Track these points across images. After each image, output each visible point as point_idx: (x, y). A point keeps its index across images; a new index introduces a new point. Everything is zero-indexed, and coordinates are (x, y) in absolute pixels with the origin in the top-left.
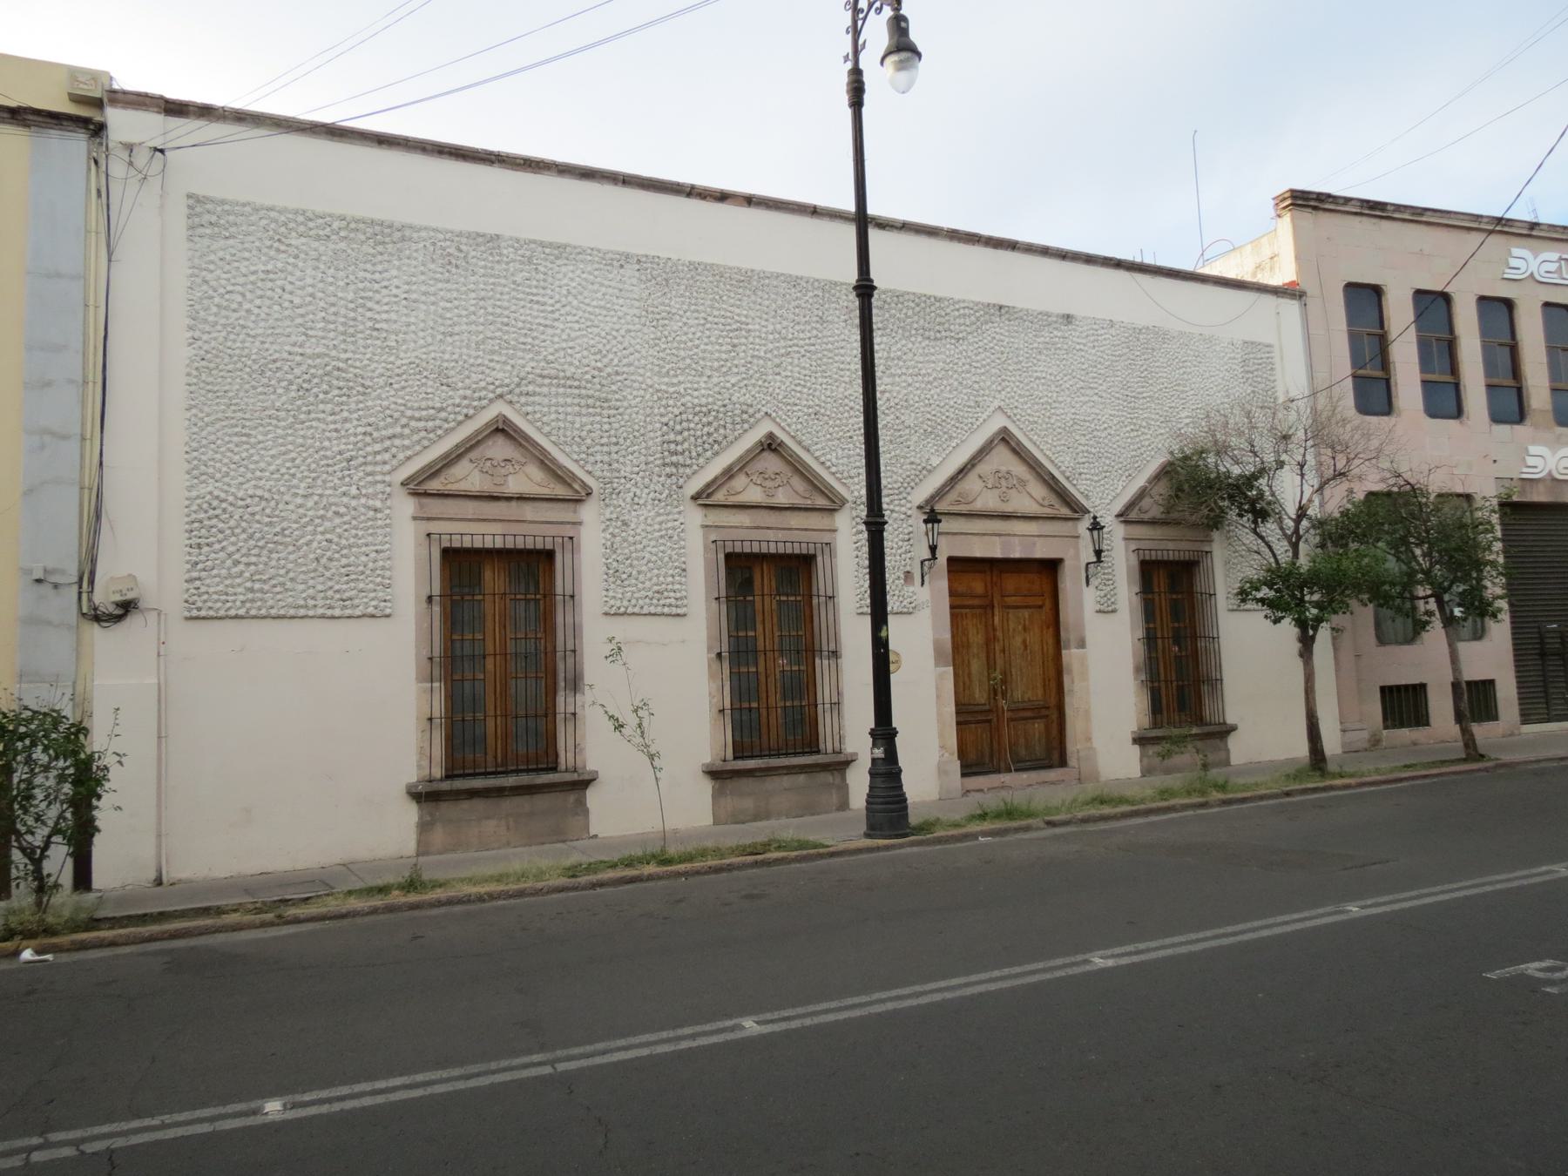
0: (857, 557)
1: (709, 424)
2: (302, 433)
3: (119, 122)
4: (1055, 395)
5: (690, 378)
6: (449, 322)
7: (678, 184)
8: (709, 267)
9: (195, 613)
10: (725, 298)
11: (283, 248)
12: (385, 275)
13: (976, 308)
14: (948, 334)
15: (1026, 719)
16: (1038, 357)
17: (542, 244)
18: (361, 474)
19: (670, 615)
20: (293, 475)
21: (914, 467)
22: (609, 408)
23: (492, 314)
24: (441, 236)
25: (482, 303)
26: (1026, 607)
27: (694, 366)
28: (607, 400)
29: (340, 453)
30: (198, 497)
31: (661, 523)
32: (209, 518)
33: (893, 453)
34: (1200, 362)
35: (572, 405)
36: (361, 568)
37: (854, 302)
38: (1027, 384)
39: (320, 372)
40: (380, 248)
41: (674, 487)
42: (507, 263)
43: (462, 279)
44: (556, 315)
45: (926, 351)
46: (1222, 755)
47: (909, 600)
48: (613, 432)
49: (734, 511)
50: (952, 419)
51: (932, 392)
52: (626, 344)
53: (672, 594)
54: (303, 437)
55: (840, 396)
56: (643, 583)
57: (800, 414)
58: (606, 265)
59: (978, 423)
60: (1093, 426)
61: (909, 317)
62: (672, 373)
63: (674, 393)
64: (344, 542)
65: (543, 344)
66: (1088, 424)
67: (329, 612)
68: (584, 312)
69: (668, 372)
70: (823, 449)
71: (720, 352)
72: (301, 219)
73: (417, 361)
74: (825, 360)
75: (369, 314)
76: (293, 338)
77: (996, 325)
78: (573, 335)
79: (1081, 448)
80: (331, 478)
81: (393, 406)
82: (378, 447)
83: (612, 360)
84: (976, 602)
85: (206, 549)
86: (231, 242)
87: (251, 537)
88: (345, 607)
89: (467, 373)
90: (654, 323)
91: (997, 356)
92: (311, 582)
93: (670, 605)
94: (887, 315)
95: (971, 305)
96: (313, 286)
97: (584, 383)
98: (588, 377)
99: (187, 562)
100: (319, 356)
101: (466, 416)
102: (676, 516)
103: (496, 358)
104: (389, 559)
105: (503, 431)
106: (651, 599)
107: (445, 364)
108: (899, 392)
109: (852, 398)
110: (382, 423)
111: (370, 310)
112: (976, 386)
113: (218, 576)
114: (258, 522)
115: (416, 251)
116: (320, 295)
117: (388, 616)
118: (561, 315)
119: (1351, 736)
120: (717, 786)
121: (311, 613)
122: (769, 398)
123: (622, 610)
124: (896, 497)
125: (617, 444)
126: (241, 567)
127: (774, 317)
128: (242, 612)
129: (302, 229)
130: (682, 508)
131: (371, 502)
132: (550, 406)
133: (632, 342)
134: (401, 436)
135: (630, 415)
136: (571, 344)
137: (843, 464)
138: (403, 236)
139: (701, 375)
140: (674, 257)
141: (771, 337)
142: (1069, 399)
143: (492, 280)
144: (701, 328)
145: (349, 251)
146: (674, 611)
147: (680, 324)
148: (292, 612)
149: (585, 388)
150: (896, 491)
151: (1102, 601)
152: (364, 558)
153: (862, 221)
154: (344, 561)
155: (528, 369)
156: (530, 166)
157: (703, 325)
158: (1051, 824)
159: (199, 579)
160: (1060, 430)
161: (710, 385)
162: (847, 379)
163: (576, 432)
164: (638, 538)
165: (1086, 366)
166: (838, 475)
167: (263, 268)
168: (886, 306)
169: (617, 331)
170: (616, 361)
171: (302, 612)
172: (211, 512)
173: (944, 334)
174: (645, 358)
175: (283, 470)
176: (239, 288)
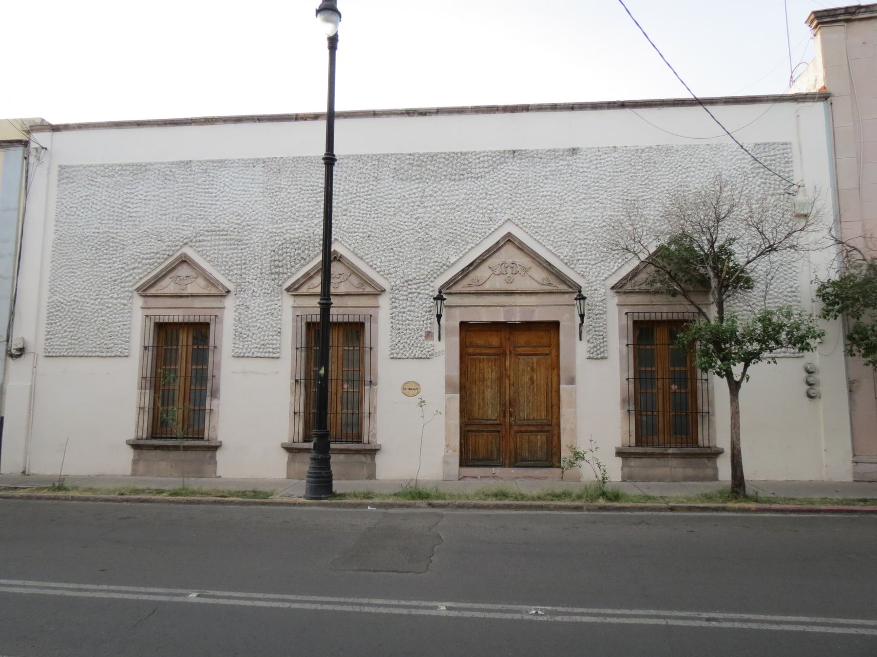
0: (392, 323)
1: (299, 248)
2: (96, 269)
3: (40, 139)
4: (558, 206)
5: (290, 223)
6: (164, 209)
7: (288, 115)
8: (304, 159)
9: (47, 354)
10: (313, 175)
11: (94, 183)
12: (137, 189)
13: (493, 155)
14: (470, 175)
15: (531, 432)
16: (545, 181)
17: (213, 162)
18: (119, 288)
19: (269, 358)
20: (91, 290)
21: (437, 264)
22: (242, 244)
23: (185, 202)
24: (163, 166)
25: (181, 197)
26: (535, 355)
27: (292, 216)
28: (241, 241)
29: (111, 278)
30: (52, 302)
31: (267, 306)
32: (56, 311)
33: (422, 257)
34: (705, 166)
35: (223, 245)
36: (116, 333)
37: (323, 169)
38: (534, 201)
39: (105, 240)
40: (135, 177)
41: (276, 286)
42: (194, 174)
43: (172, 186)
44: (217, 198)
45: (452, 188)
46: (709, 472)
47: (427, 350)
48: (243, 258)
49: (312, 297)
50: (469, 231)
51: (455, 214)
52: (254, 209)
53: (271, 346)
54: (97, 271)
55: (386, 224)
56: (255, 340)
57: (358, 237)
58: (245, 167)
59: (490, 232)
60: (592, 225)
61: (441, 168)
62: (279, 221)
63: (279, 233)
64: (110, 321)
65: (210, 214)
66: (588, 224)
67: (101, 354)
68: (232, 194)
69: (277, 221)
70: (372, 257)
71: (309, 206)
72: (102, 168)
73: (148, 230)
74: (377, 203)
75: (128, 210)
76: (95, 225)
77: (509, 164)
78: (226, 207)
79: (580, 241)
80: (106, 290)
81: (135, 253)
82: (127, 274)
83: (246, 218)
84: (492, 351)
85: (54, 325)
86: (73, 184)
87: (72, 319)
88: (108, 352)
89: (170, 233)
90: (271, 195)
91: (509, 184)
92: (95, 340)
93: (269, 352)
94: (424, 169)
95: (489, 154)
96: (105, 200)
97: (229, 232)
98: (232, 229)
99: (46, 331)
100: (105, 232)
101: (168, 255)
102: (277, 302)
103: (185, 224)
104: (129, 328)
105: (185, 261)
106: (260, 349)
107: (161, 230)
108: (429, 217)
109: (394, 224)
110: (129, 263)
111: (129, 207)
112: (490, 207)
113: (58, 337)
114: (75, 312)
115: (151, 175)
116: (108, 203)
117: (127, 356)
118: (220, 198)
119: (862, 468)
120: (290, 457)
121: (94, 355)
122: (338, 230)
123: (242, 354)
124: (422, 284)
125: (245, 264)
126: (67, 333)
127: (344, 182)
128: (65, 354)
129: (103, 173)
130: (280, 297)
131: (122, 301)
132: (211, 246)
133: (258, 207)
134: (138, 268)
135: (254, 247)
136: (224, 212)
137: (385, 266)
138: (146, 169)
139: (297, 221)
140: (285, 156)
141: (342, 194)
142: (571, 208)
143: (186, 184)
144: (298, 194)
145: (121, 181)
146: (271, 355)
147: (286, 193)
148: (86, 354)
149: (230, 235)
150: (422, 281)
151: (592, 351)
152: (118, 328)
153: (331, 116)
154: (109, 330)
155: (201, 228)
156: (208, 122)
157: (300, 192)
158: (431, 505)
159: (50, 339)
160: (560, 231)
161: (302, 226)
162: (392, 213)
163: (224, 259)
164: (254, 315)
165: (589, 182)
166: (382, 273)
167: (85, 194)
168: (423, 164)
169: (250, 202)
170: (248, 218)
171: (90, 354)
172: (57, 308)
173: (466, 175)
174: (265, 215)
175: (87, 288)
176: (75, 205)
